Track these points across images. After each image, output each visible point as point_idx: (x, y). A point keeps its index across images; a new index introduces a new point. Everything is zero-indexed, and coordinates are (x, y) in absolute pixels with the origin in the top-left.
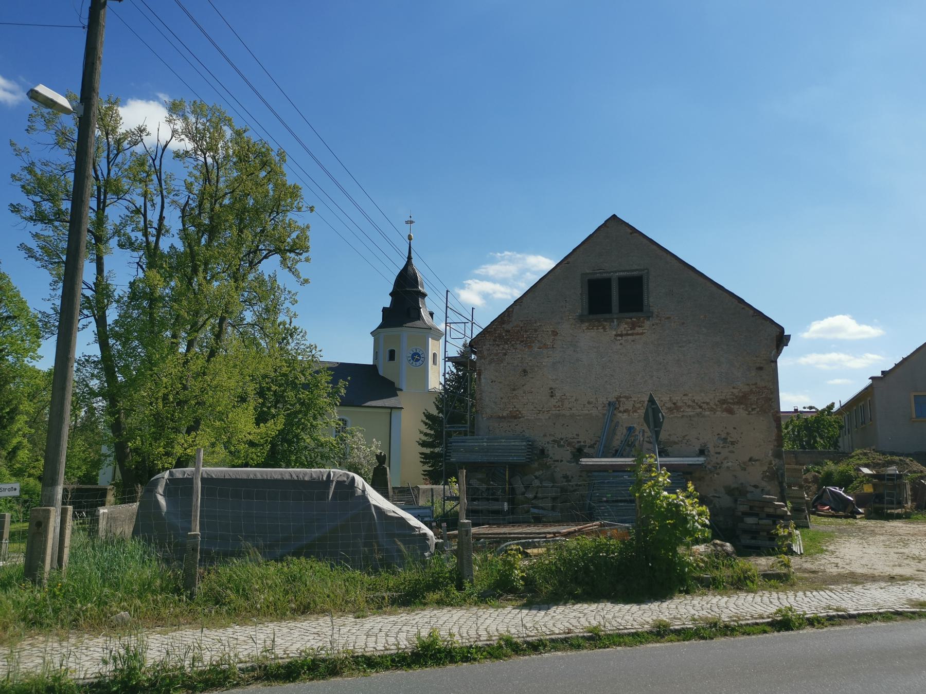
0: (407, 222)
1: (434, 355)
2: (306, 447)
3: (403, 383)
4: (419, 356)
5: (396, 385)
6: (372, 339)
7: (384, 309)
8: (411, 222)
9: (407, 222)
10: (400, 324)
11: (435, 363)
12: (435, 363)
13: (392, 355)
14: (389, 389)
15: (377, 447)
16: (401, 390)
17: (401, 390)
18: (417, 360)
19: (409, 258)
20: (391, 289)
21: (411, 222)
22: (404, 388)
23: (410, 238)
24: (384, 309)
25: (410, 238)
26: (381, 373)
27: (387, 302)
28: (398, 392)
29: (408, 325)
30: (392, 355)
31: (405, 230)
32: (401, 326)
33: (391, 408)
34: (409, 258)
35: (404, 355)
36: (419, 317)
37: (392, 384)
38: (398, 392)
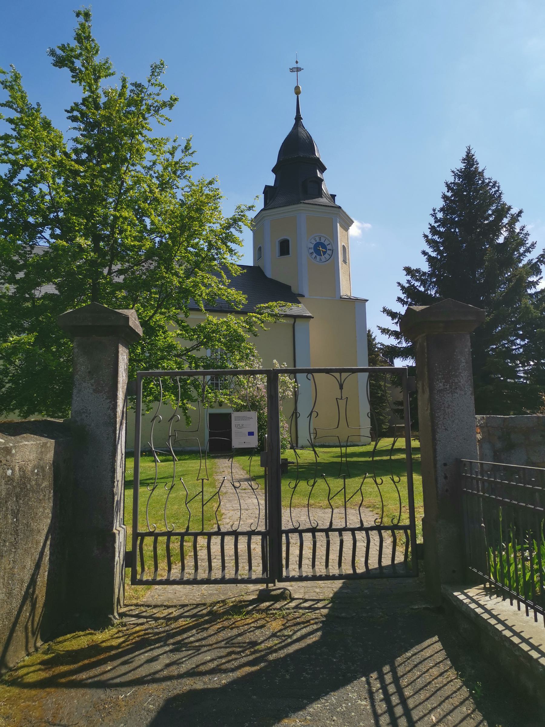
0: (292, 70)
4: (324, 246)
5: (294, 290)
7: (267, 187)
8: (298, 69)
9: (292, 70)
11: (345, 261)
12: (345, 261)
13: (284, 248)
16: (303, 296)
17: (303, 296)
19: (298, 118)
20: (274, 162)
21: (298, 69)
22: (306, 293)
23: (297, 91)
24: (268, 191)
25: (297, 91)
26: (269, 274)
27: (271, 180)
28: (300, 299)
29: (306, 201)
30: (284, 248)
31: (291, 79)
32: (298, 202)
34: (298, 118)
35: (302, 245)
36: (319, 193)
37: (289, 287)
38: (300, 299)
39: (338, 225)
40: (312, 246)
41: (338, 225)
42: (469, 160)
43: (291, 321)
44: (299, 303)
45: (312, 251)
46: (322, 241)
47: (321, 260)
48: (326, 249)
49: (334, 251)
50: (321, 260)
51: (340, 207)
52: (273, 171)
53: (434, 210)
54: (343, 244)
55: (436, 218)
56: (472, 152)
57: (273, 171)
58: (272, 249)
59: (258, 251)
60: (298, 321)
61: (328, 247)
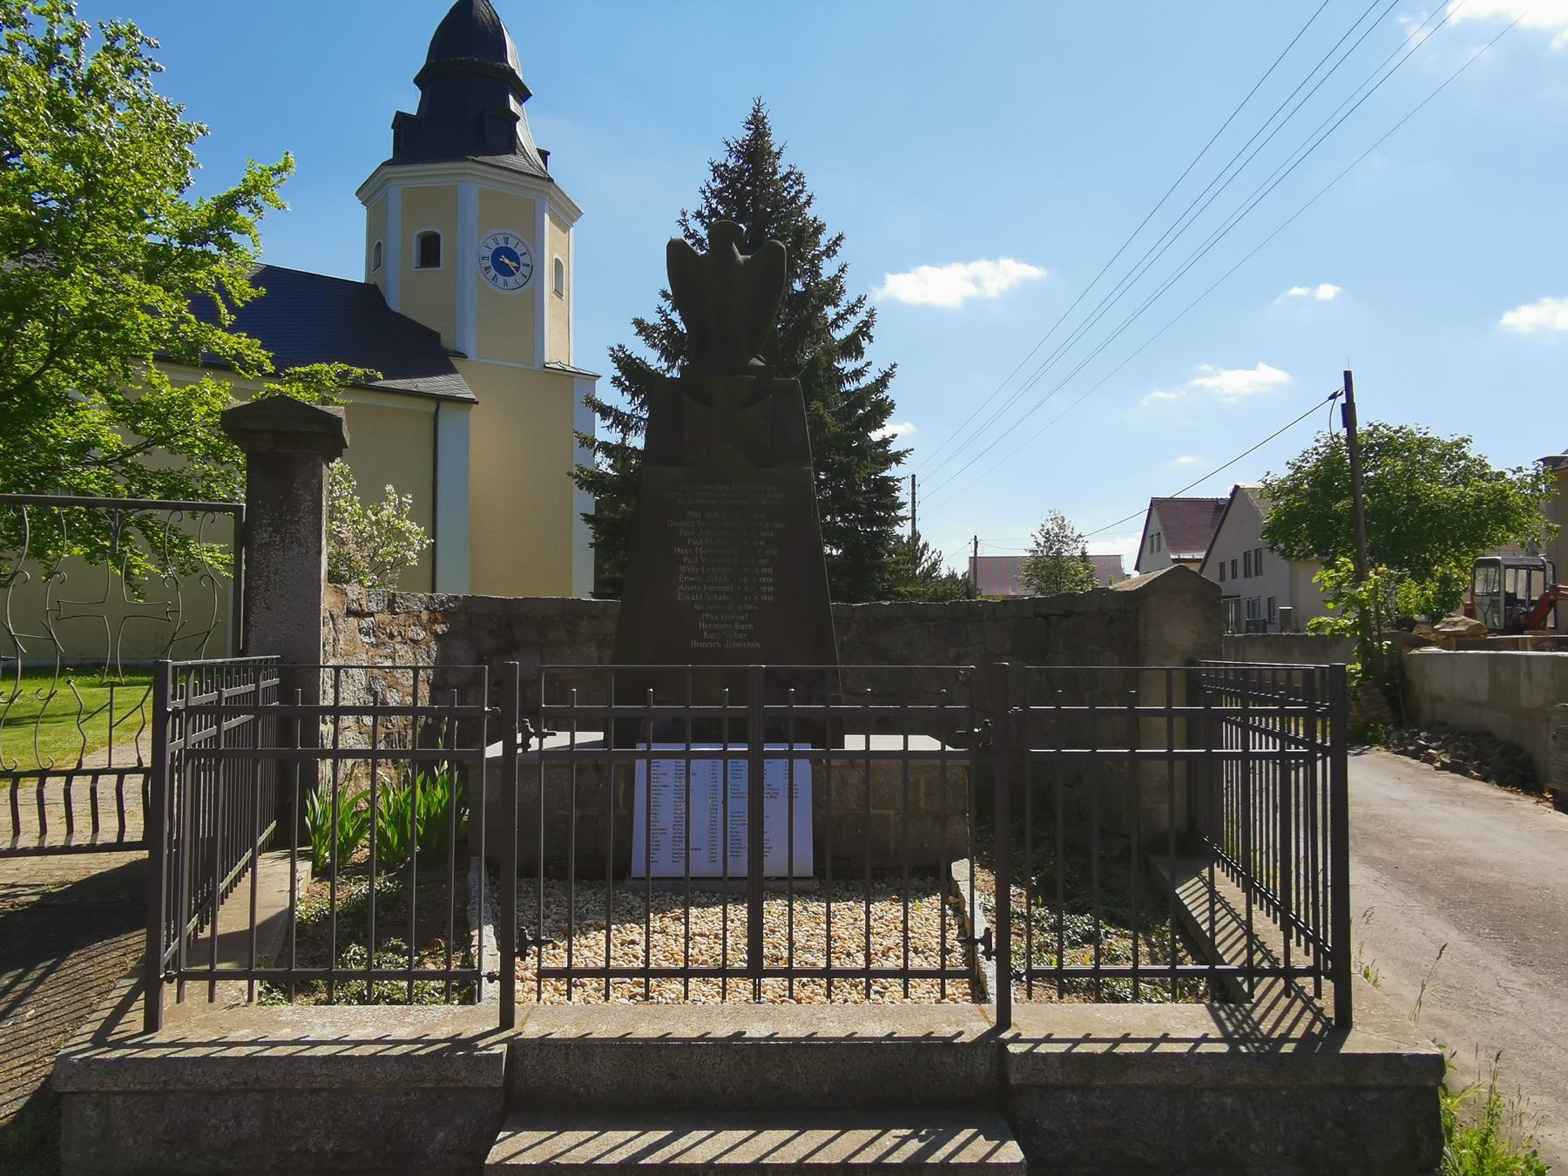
1: (558, 263)
2: (81, 450)
3: (468, 336)
4: (513, 256)
5: (445, 341)
6: (359, 215)
7: (399, 114)
10: (456, 152)
11: (558, 292)
12: (558, 292)
13: (430, 250)
14: (425, 350)
15: (400, 507)
16: (463, 356)
17: (463, 356)
18: (507, 272)
22: (471, 349)
24: (401, 122)
26: (395, 305)
27: (411, 102)
28: (456, 362)
29: (480, 159)
30: (430, 250)
33: (439, 399)
35: (469, 249)
36: (510, 143)
37: (435, 336)
39: (547, 217)
40: (489, 254)
41: (547, 217)
42: (757, 124)
43: (430, 407)
44: (453, 371)
45: (489, 263)
46: (511, 245)
47: (506, 283)
48: (518, 261)
49: (535, 270)
50: (506, 283)
51: (551, 180)
52: (417, 81)
53: (684, 214)
54: (556, 256)
55: (687, 229)
56: (764, 111)
57: (417, 81)
58: (403, 251)
59: (376, 254)
60: (445, 409)
61: (523, 260)
